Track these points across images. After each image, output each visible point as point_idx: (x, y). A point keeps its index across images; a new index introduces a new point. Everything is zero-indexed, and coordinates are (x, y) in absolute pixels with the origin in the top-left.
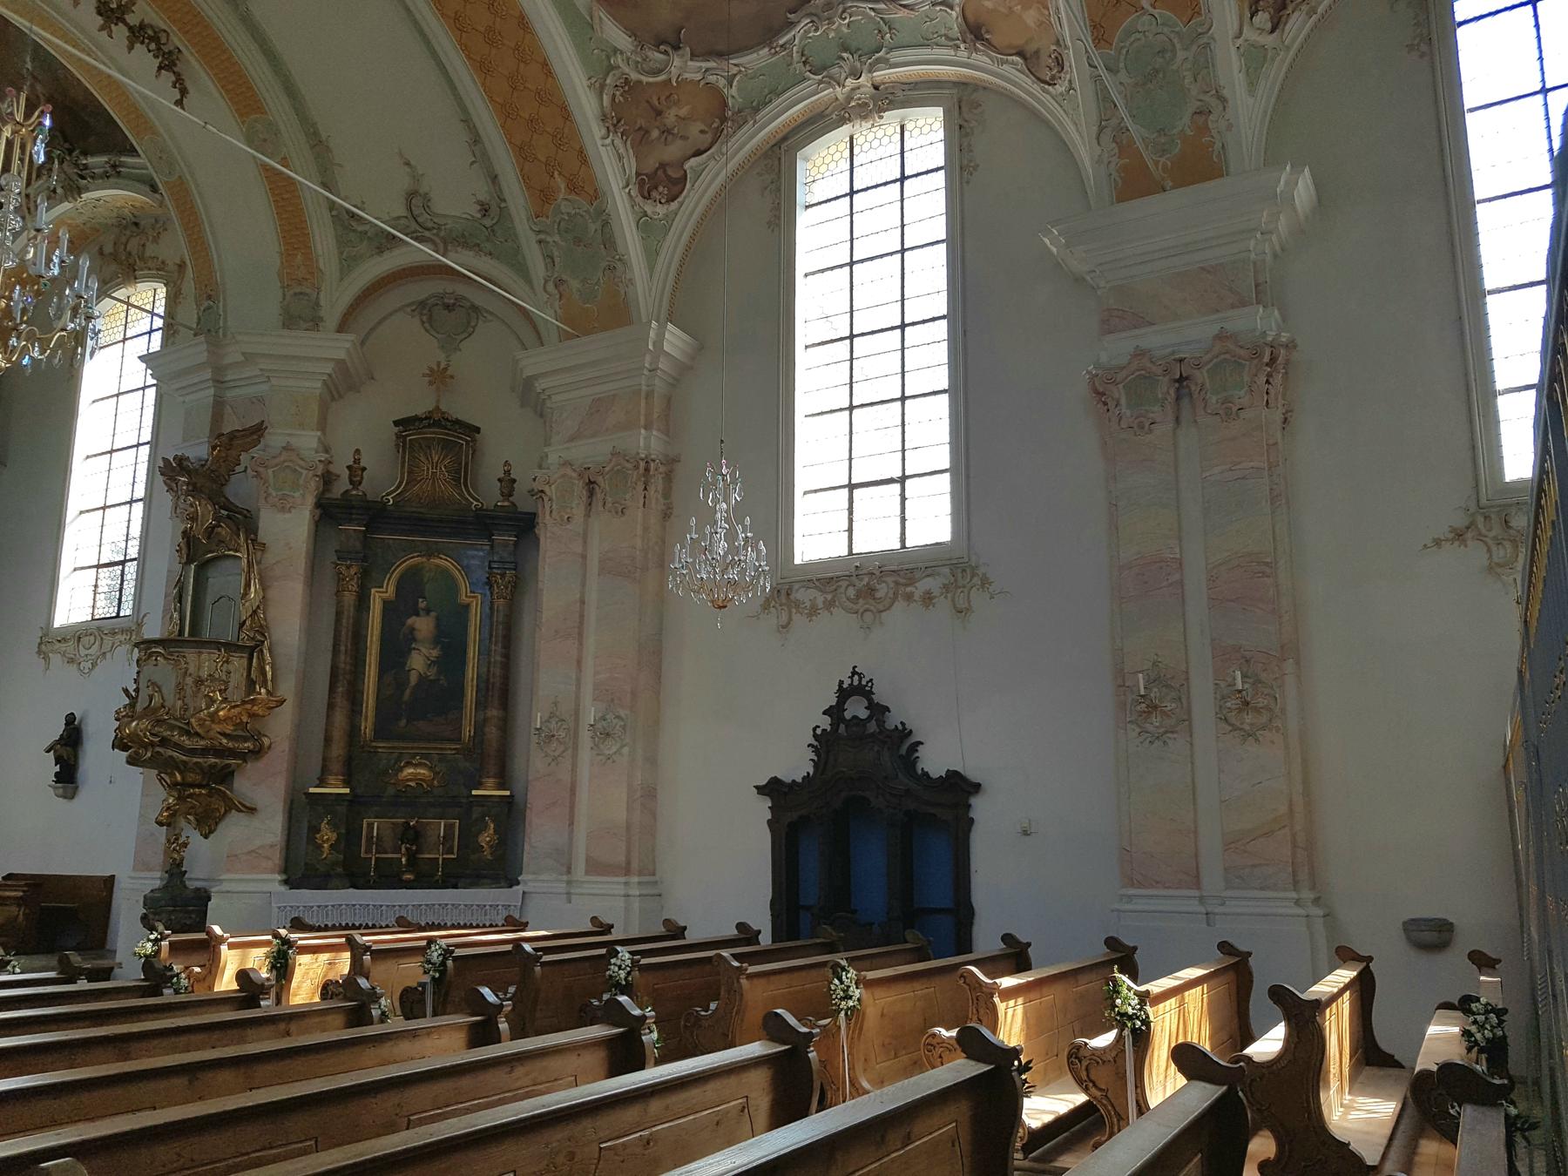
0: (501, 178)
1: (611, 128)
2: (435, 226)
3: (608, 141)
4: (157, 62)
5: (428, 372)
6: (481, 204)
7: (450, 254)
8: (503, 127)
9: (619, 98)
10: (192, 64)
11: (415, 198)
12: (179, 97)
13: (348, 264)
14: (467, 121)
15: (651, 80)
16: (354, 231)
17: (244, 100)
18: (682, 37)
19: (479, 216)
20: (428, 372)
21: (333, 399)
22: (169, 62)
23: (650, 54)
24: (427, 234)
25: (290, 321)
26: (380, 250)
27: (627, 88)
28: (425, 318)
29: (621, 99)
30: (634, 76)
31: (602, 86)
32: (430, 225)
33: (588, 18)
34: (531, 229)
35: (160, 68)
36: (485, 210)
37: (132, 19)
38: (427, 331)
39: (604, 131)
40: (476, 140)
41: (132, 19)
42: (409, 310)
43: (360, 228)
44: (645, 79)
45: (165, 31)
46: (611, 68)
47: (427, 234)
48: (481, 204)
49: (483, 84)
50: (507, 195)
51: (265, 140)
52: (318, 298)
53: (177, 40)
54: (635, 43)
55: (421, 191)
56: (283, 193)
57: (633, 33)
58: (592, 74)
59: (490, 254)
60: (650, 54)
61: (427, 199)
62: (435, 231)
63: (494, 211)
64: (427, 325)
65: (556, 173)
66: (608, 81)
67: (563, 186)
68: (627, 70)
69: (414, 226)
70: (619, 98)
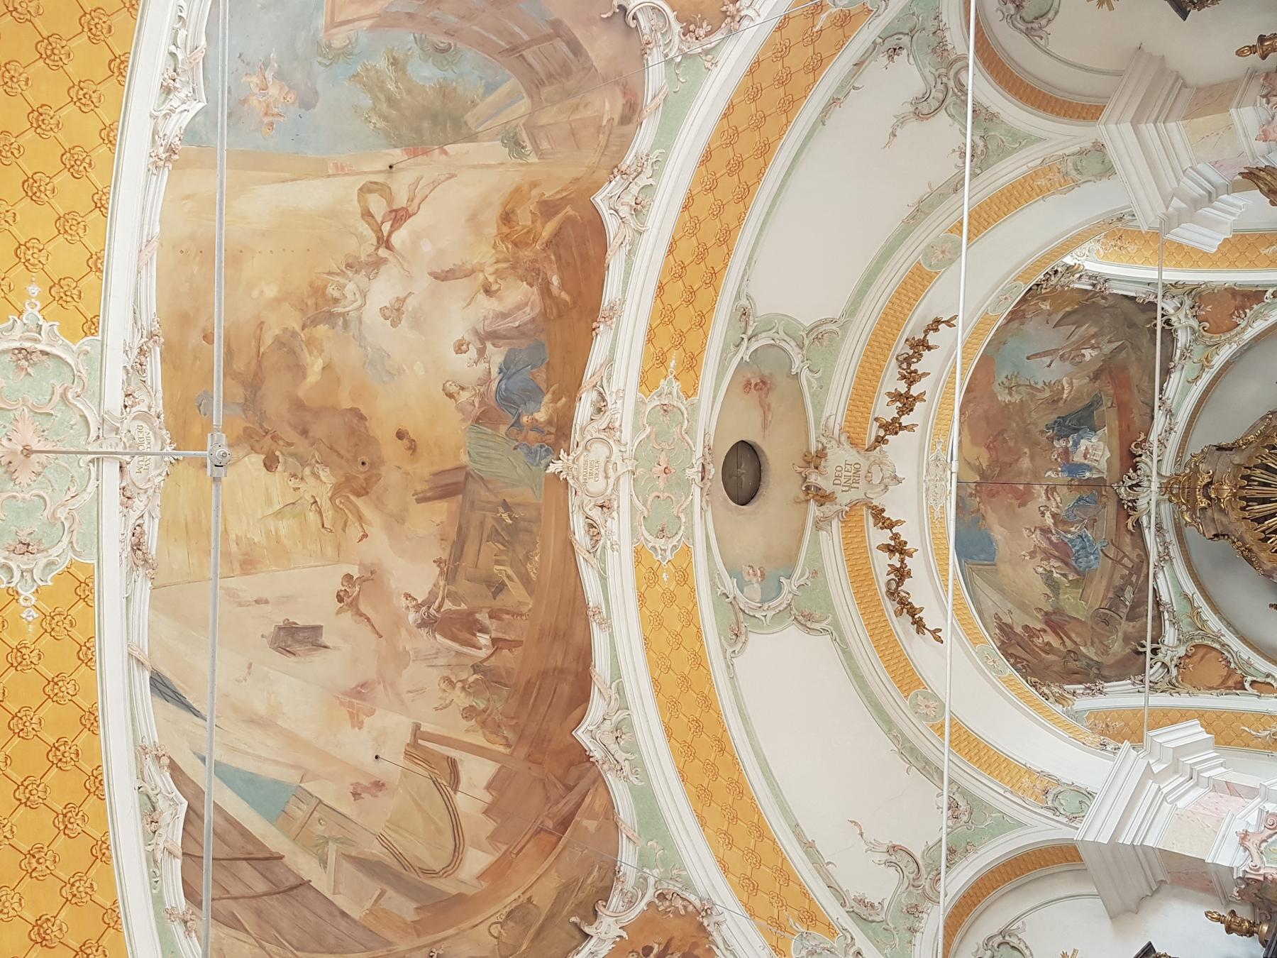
0: (854, 61)
1: (737, 19)
2: (939, 81)
3: (751, 12)
4: (926, 353)
5: (1105, 6)
6: (891, 58)
7: (960, 50)
8: (806, 97)
9: (706, 27)
10: (913, 327)
11: (921, 110)
12: (943, 324)
13: (1023, 140)
14: (822, 120)
15: (668, 10)
16: (986, 146)
17: (919, 281)
18: (609, 14)
19: (904, 52)
20: (1105, 6)
21: (1185, 85)
22: (920, 346)
23: (647, 31)
24: (951, 84)
25: (1108, 170)
26: (992, 117)
27: (692, 27)
28: (1044, 22)
29: (705, 25)
30: (677, 28)
31: (707, 52)
32: (940, 87)
33: (661, 108)
34: (886, 9)
35: (929, 348)
36: (896, 50)
37: (902, 387)
38: (1057, 12)
39: (745, 23)
40: (834, 101)
41: (902, 387)
42: (1042, 42)
43: (981, 143)
44: (671, 15)
45: (897, 359)
46: (685, 56)
47: (951, 84)
48: (891, 58)
49: (780, 138)
50: (868, 44)
51: (943, 252)
52: (1073, 155)
53: (901, 348)
54: (648, 51)
55: (912, 109)
56: (984, 218)
57: (643, 66)
58: (704, 69)
59: (936, 17)
60: (647, 31)
61: (917, 101)
62: (945, 80)
63: (891, 43)
64: (1050, 15)
65: (815, 30)
66: (700, 50)
67: (824, 16)
68: (676, 40)
69: (950, 99)
70: (706, 27)
